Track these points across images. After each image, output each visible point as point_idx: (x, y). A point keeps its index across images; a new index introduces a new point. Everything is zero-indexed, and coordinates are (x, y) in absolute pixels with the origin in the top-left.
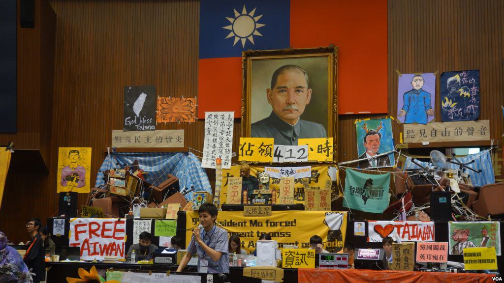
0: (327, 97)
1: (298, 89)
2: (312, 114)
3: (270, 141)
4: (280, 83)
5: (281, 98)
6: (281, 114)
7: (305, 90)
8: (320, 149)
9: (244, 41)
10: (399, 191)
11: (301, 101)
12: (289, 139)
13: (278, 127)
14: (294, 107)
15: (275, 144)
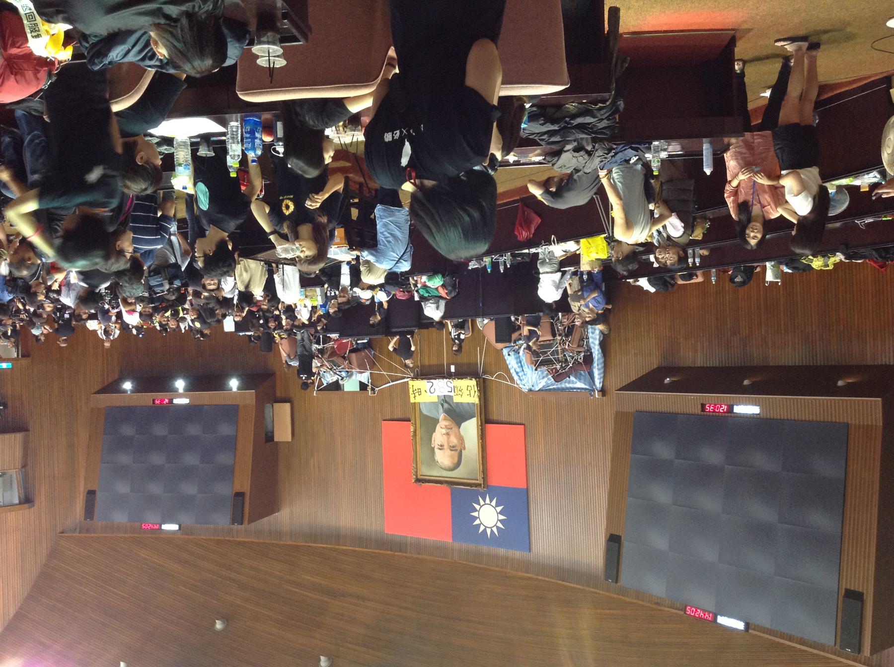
0: (421, 438)
1: (441, 447)
2: (431, 424)
3: (457, 399)
4: (456, 454)
5: (454, 441)
6: (453, 425)
7: (436, 447)
8: (419, 391)
9: (488, 501)
10: (353, 356)
11: (439, 436)
12: (446, 402)
13: (457, 414)
14: (444, 431)
15: (451, 397)
